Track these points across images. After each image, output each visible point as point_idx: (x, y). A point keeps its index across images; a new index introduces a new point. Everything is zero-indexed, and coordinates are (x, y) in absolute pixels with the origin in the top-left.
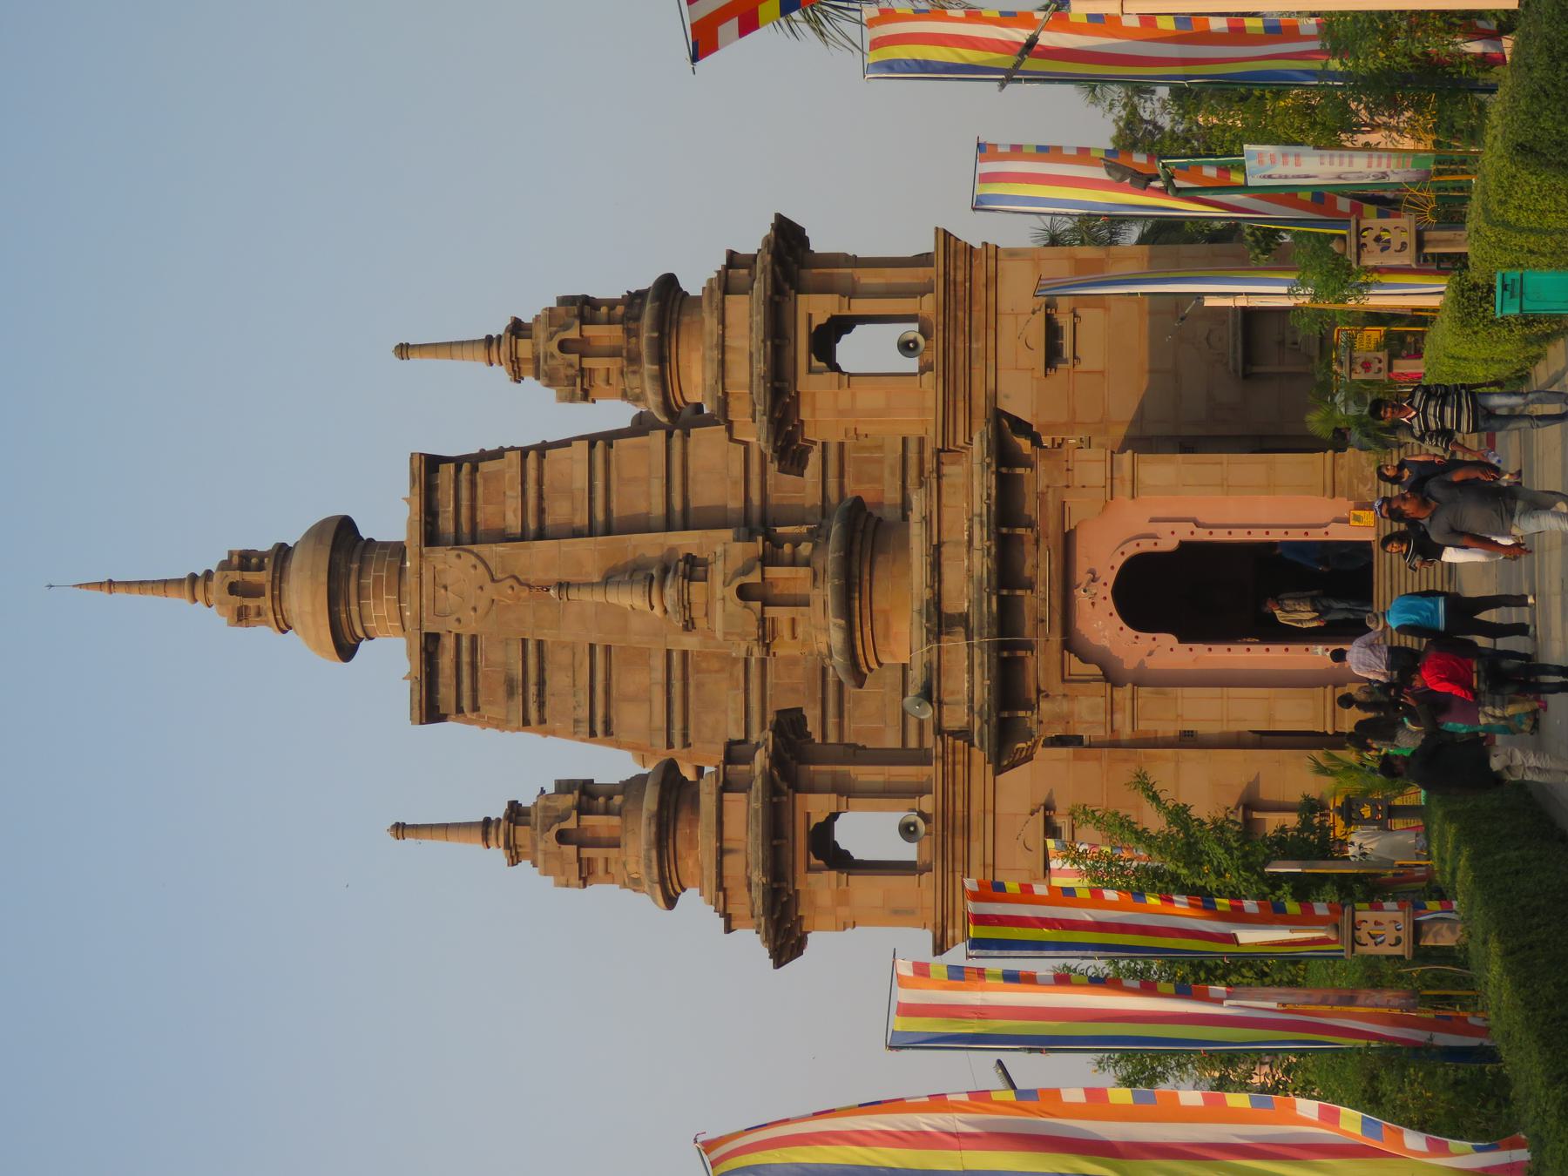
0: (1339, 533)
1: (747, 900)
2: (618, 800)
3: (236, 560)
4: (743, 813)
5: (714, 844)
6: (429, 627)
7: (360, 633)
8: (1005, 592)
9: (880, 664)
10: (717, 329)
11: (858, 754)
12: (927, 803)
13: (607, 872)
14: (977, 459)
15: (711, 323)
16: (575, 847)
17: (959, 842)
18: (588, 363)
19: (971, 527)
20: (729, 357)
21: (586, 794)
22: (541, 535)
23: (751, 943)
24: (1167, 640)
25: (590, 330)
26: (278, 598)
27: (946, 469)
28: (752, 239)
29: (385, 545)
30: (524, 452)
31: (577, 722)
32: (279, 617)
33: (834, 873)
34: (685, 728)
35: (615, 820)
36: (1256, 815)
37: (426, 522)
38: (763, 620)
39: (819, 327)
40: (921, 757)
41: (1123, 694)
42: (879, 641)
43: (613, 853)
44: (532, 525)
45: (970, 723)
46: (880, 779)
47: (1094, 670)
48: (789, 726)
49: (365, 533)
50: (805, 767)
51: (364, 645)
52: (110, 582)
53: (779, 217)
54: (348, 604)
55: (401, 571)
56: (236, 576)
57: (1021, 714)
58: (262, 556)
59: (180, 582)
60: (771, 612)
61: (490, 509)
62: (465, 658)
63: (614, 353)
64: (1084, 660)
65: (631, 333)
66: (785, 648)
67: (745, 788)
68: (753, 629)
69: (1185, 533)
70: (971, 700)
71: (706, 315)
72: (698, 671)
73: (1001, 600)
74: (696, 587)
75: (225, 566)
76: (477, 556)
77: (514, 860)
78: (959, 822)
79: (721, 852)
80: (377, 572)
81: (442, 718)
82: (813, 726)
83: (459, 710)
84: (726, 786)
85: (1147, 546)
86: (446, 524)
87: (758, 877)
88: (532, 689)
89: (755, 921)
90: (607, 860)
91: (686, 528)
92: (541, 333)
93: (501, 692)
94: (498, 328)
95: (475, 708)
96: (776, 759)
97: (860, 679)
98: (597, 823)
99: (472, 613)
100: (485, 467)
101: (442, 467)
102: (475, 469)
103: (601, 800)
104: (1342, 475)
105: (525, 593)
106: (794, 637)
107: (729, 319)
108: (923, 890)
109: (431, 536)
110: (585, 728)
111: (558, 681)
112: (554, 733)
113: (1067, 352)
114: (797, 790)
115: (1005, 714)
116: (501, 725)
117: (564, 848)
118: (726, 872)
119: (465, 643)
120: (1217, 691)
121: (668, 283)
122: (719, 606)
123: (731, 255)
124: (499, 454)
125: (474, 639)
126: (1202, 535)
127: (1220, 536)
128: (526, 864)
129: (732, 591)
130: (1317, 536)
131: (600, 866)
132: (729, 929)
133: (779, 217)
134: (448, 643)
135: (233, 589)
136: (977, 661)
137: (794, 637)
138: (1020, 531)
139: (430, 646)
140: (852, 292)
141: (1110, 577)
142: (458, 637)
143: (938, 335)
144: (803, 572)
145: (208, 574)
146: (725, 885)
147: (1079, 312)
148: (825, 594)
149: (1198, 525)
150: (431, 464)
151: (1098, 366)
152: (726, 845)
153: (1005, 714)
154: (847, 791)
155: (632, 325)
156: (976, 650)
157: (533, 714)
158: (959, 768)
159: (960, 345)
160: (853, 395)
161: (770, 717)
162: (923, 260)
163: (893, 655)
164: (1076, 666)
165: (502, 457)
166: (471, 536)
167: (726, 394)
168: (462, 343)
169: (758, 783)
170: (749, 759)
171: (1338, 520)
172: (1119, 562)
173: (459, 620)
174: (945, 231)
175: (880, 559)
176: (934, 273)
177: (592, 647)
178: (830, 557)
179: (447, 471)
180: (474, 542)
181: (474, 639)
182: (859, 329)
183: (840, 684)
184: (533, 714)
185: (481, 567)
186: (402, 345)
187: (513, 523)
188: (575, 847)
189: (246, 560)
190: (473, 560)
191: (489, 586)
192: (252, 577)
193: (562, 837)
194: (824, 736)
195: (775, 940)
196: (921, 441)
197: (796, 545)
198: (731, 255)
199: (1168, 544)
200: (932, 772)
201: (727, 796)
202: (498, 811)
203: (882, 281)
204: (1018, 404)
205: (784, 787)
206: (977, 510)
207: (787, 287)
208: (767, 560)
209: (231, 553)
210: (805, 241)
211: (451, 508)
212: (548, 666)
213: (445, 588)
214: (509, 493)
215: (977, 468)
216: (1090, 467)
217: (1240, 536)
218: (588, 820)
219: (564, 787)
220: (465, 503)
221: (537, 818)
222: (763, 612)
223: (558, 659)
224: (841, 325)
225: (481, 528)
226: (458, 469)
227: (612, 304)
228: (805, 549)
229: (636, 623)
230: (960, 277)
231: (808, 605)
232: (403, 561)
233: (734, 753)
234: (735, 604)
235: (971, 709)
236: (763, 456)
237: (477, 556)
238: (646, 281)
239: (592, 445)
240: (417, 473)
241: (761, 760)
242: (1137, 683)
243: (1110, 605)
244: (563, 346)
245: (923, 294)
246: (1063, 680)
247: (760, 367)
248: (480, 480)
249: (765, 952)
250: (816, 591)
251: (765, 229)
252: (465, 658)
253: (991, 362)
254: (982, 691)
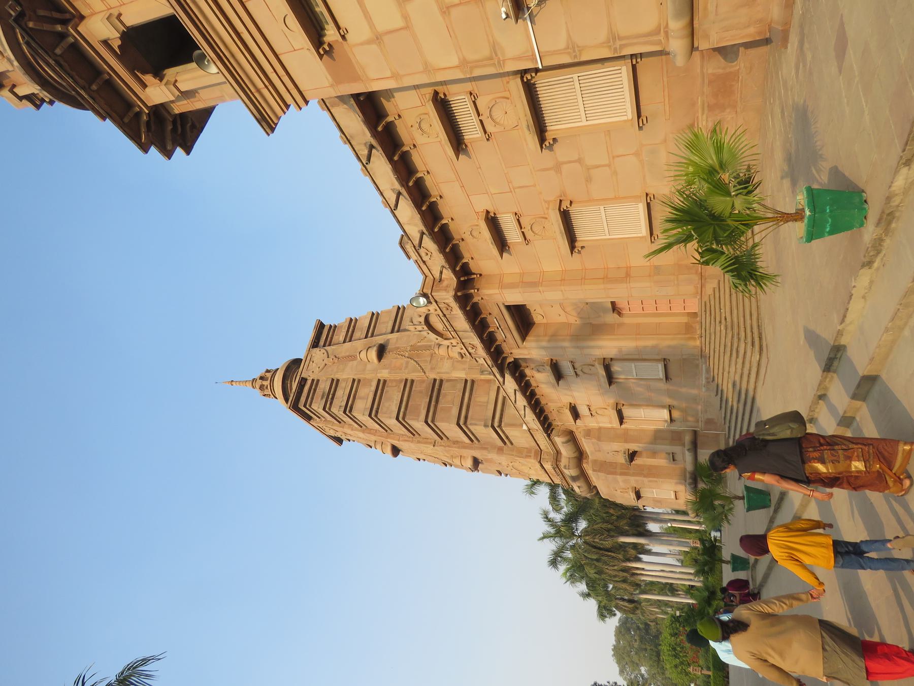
31: (340, 406)
32: (272, 388)
34: (378, 408)
37: (315, 342)
54: (291, 381)
72: (387, 387)
76: (326, 350)
88: (330, 396)
99: (318, 369)
105: (336, 360)
111: (339, 393)
125: (318, 381)
134: (309, 382)
177: (354, 380)
185: (326, 353)
189: (268, 371)
190: (324, 351)
191: (326, 359)
211: (324, 338)
213: (313, 362)
214: (343, 330)
223: (342, 385)
229: (369, 367)
237: (326, 350)
240: (317, 324)
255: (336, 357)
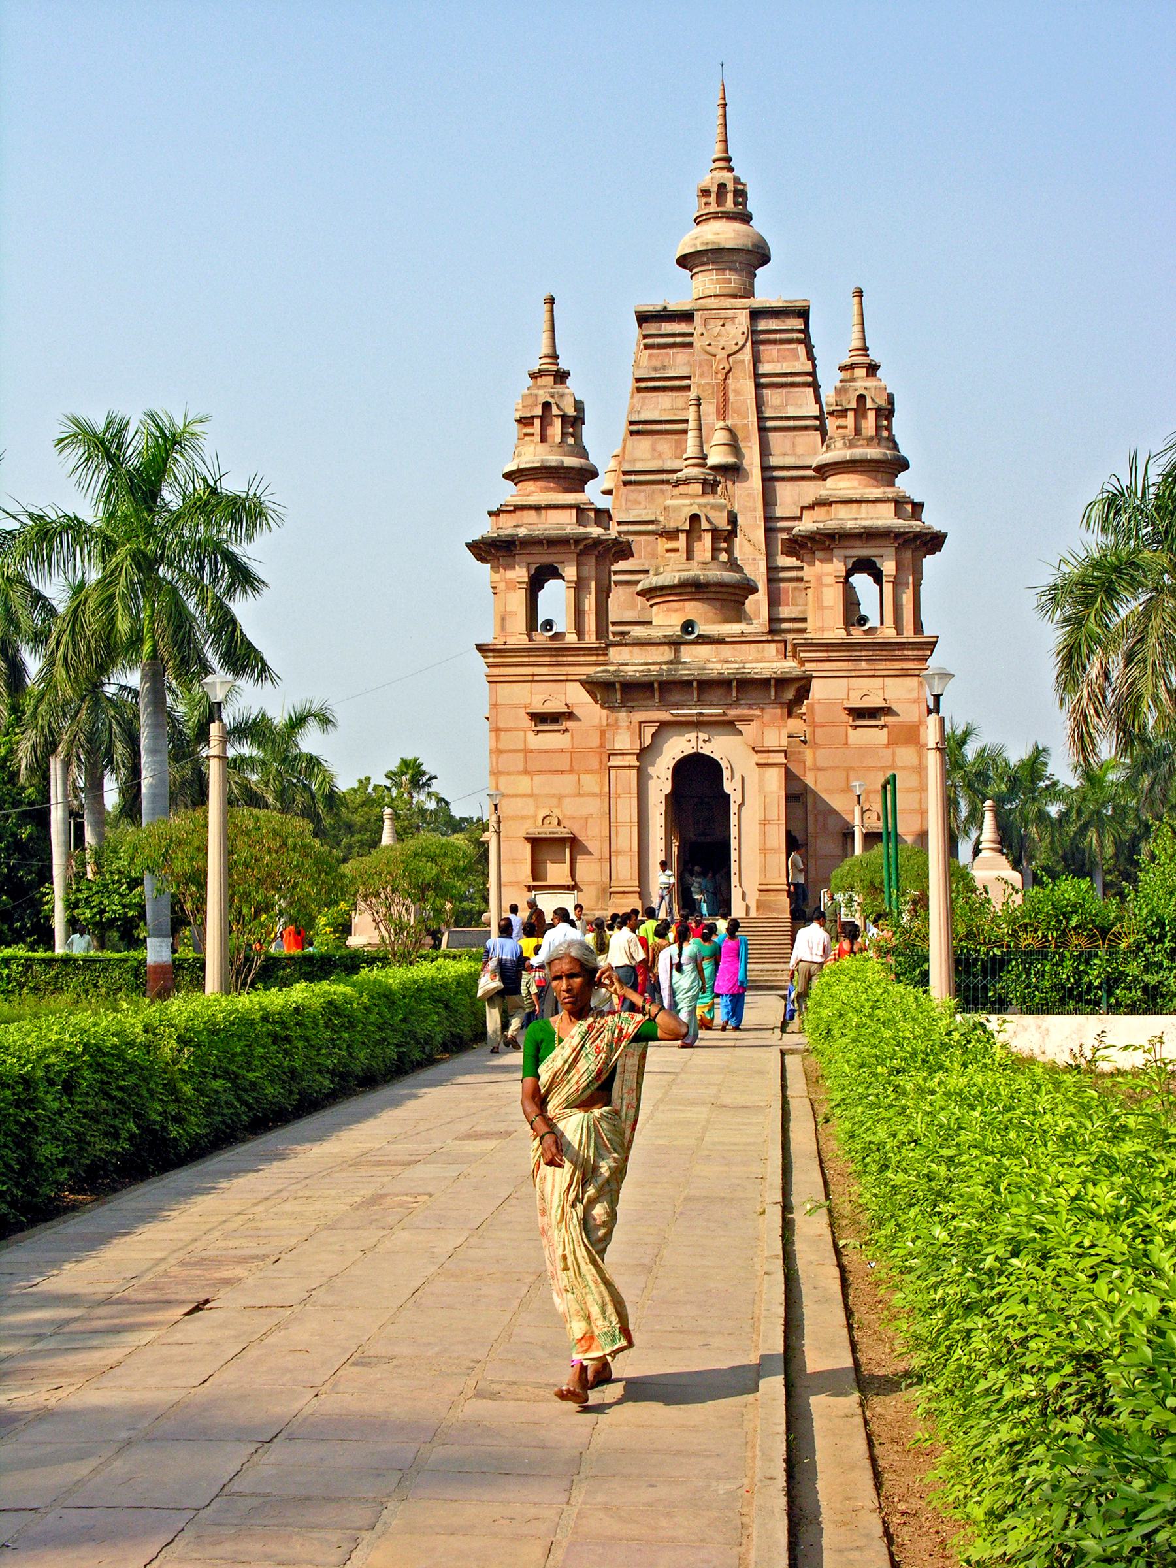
0: (736, 894)
1: (507, 527)
2: (571, 441)
3: (740, 187)
4: (563, 523)
5: (543, 503)
6: (698, 316)
7: (695, 271)
8: (695, 684)
9: (651, 606)
10: (872, 497)
11: (603, 595)
12: (571, 638)
13: (526, 435)
14: (779, 665)
15: (877, 492)
16: (540, 413)
17: (548, 659)
18: (851, 414)
19: (735, 662)
20: (855, 505)
21: (573, 422)
22: (758, 386)
23: (485, 528)
24: (668, 788)
25: (871, 415)
26: (716, 216)
27: (773, 645)
28: (931, 520)
29: (752, 285)
30: (813, 374)
33: (526, 580)
35: (558, 439)
36: (568, 844)
38: (678, 531)
39: (874, 563)
40: (601, 632)
41: (633, 761)
42: (665, 606)
43: (537, 438)
44: (763, 380)
45: (611, 664)
46: (587, 608)
47: (648, 742)
48: (622, 550)
49: (759, 272)
50: (593, 560)
51: (687, 273)
52: (725, 105)
53: (944, 536)
55: (734, 296)
56: (730, 187)
57: (619, 697)
58: (744, 204)
59: (726, 151)
60: (683, 537)
61: (775, 354)
62: (679, 340)
63: (858, 431)
64: (654, 735)
65: (871, 439)
66: (663, 544)
67: (580, 521)
68: (672, 525)
69: (735, 798)
70: (626, 664)
71: (882, 490)
73: (690, 683)
74: (698, 488)
75: (737, 180)
76: (744, 345)
77: (534, 376)
78: (560, 659)
79: (537, 508)
80: (734, 280)
81: (640, 326)
82: (622, 565)
83: (645, 337)
84: (580, 510)
85: (726, 774)
86: (763, 325)
87: (522, 532)
89: (495, 529)
90: (533, 435)
91: (764, 480)
92: (871, 383)
93: (658, 364)
94: (874, 356)
95: (647, 347)
96: (597, 542)
97: (645, 593)
98: (556, 429)
100: (801, 349)
101: (801, 321)
102: (799, 341)
103: (571, 430)
104: (771, 897)
105: (721, 377)
106: (668, 551)
107: (879, 505)
108: (517, 635)
109: (756, 315)
110: (635, 418)
112: (632, 397)
113: (858, 723)
114: (578, 555)
115: (618, 686)
116: (637, 364)
117: (540, 407)
118: (525, 512)
119: (688, 339)
120: (635, 819)
121: (903, 465)
122: (687, 502)
123: (921, 505)
124: (811, 357)
125: (690, 345)
126: (734, 808)
127: (734, 820)
128: (530, 382)
129: (695, 510)
130: (734, 880)
131: (529, 430)
132: (491, 514)
133: (944, 536)
135: (722, 186)
136: (652, 668)
137: (668, 551)
138: (734, 694)
139: (687, 316)
140: (897, 584)
141: (706, 750)
142: (691, 335)
143: (868, 639)
144: (709, 555)
145: (731, 170)
146: (518, 513)
147: (885, 730)
148: (695, 571)
149: (741, 805)
150: (803, 314)
151: (850, 741)
152: (543, 512)
153: (618, 686)
154: (579, 587)
155: (875, 441)
156: (657, 667)
157: (643, 385)
158: (594, 658)
159: (863, 653)
160: (831, 585)
161: (624, 538)
162: (918, 627)
163: (657, 614)
164: (650, 730)
165: (809, 359)
166: (756, 339)
167: (831, 504)
168: (863, 331)
169: (582, 530)
170: (598, 523)
171: (744, 894)
172: (716, 756)
173: (702, 334)
174: (936, 642)
175: (718, 604)
176: (908, 634)
178: (716, 574)
179: (798, 324)
180: (753, 343)
181: (690, 345)
182: (878, 588)
183: (637, 582)
184: (643, 385)
185: (737, 348)
186: (862, 292)
187: (764, 368)
188: (540, 413)
189: (741, 194)
190: (741, 343)
191: (723, 354)
192: (730, 197)
193: (547, 406)
194: (616, 573)
195: (484, 544)
196: (803, 631)
197: (726, 551)
198: (921, 505)
199: (728, 787)
200: (591, 639)
201: (574, 512)
202: (563, 365)
203: (904, 602)
204: (818, 689)
205: (581, 547)
206: (747, 665)
207: (900, 541)
208: (715, 531)
209: (744, 185)
210: (932, 551)
212: (674, 394)
214: (785, 364)
215: (774, 665)
216: (775, 737)
217: (734, 832)
218: (558, 423)
219: (579, 406)
220: (778, 336)
221: (560, 388)
222: (682, 531)
224: (878, 577)
225: (762, 347)
226: (800, 331)
227: (889, 428)
228: (724, 557)
230: (906, 653)
231: (688, 559)
232: (741, 297)
233: (603, 516)
234: (687, 513)
235: (623, 665)
236: (792, 529)
237: (744, 345)
238: (904, 451)
239: (816, 418)
241: (595, 531)
242: (639, 768)
243: (690, 751)
244: (861, 398)
245: (896, 628)
246: (641, 723)
247: (850, 525)
248: (793, 346)
249: (477, 537)
250: (695, 564)
251: (937, 527)
252: (679, 340)
253: (853, 673)
254: (632, 672)
255: (729, 372)
